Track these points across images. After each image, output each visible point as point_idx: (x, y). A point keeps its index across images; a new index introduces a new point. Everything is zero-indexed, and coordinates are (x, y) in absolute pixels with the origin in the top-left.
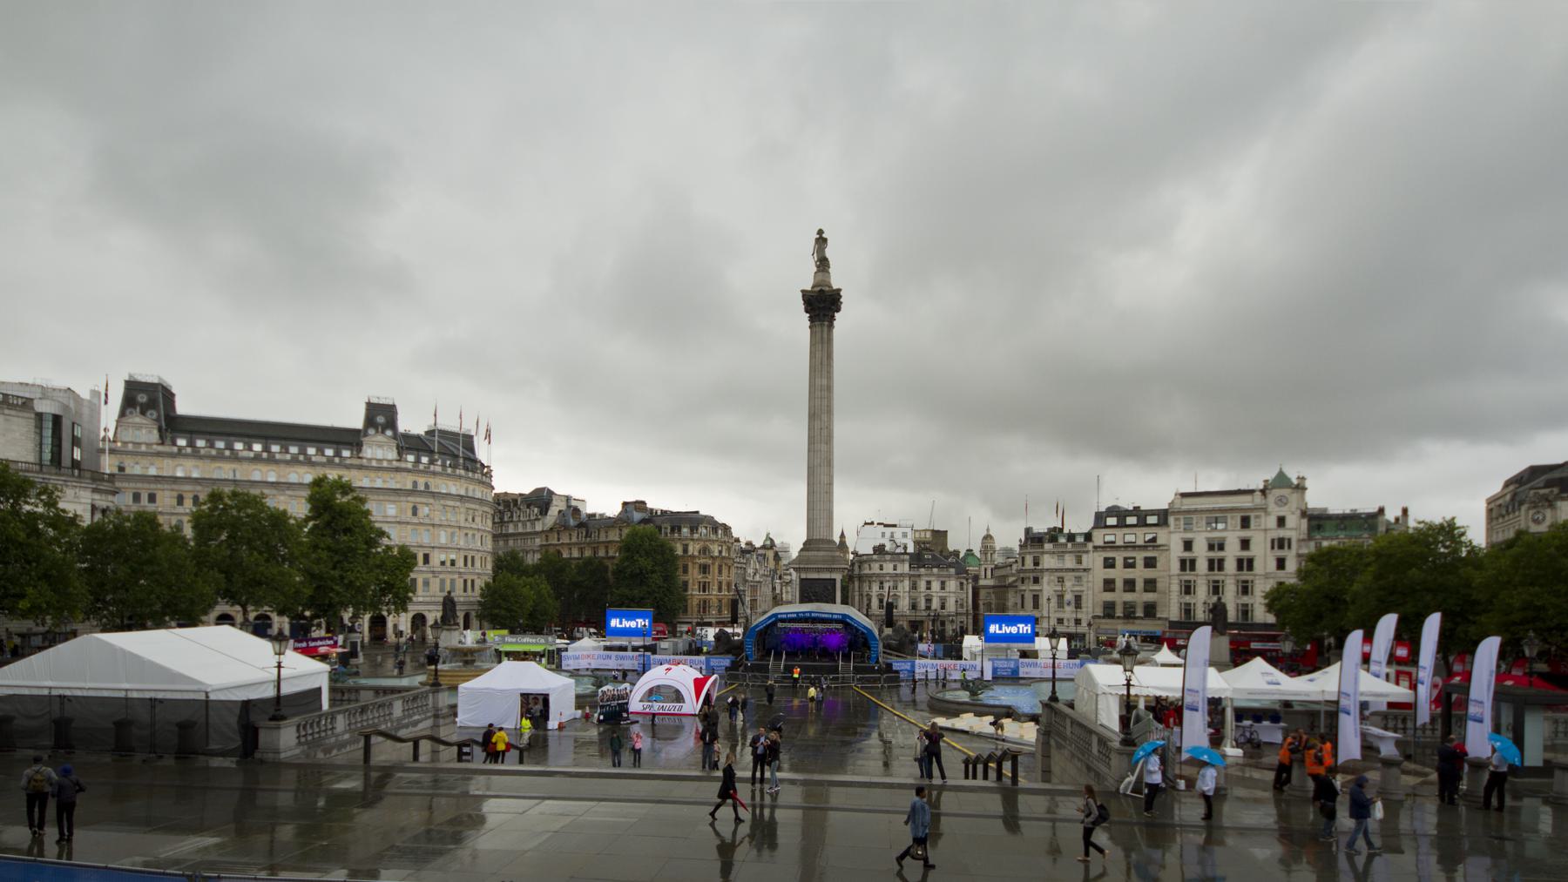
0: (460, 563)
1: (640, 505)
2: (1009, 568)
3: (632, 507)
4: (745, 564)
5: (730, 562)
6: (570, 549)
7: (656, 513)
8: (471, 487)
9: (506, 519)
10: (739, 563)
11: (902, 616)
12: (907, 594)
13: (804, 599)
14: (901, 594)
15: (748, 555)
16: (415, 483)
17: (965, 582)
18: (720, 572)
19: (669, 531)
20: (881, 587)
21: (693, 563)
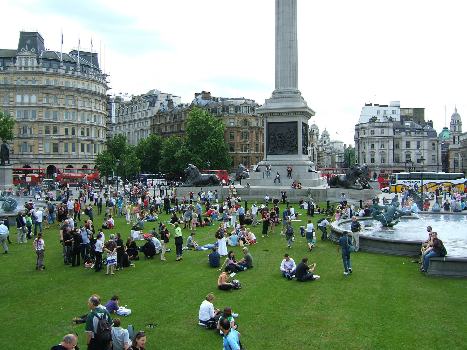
0: (79, 133)
1: (206, 95)
3: (199, 97)
6: (166, 127)
7: (217, 100)
8: (86, 84)
9: (133, 111)
11: (388, 167)
12: (392, 151)
14: (387, 151)
16: (48, 80)
17: (436, 143)
18: (257, 138)
19: (221, 110)
20: (373, 147)
21: (238, 132)
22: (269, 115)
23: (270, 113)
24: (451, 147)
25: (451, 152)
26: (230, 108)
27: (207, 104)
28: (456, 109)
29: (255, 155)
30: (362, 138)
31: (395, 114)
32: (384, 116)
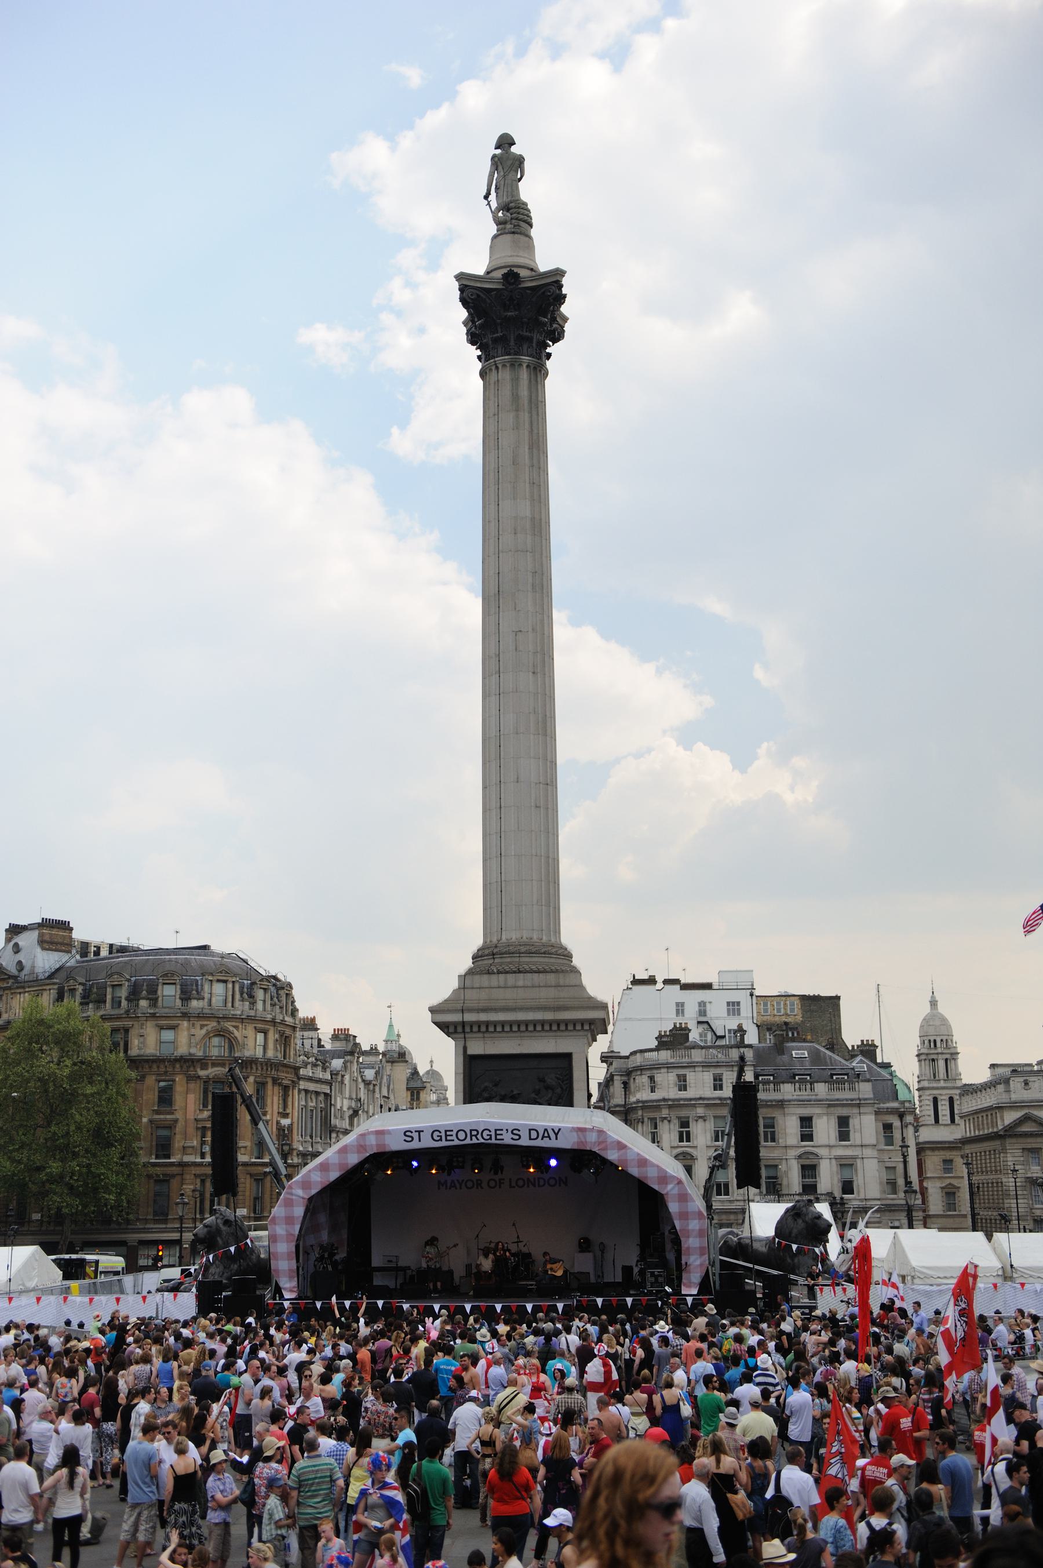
2: (1001, 1088)
4: (329, 1083)
5: (286, 1078)
7: (97, 953)
10: (310, 1079)
13: (472, 1094)
15: (337, 1063)
17: (897, 1123)
19: (123, 993)
20: (685, 1136)
21: (190, 1078)
22: (475, 1029)
23: (479, 1024)
24: (928, 1134)
25: (928, 1152)
26: (160, 987)
27: (58, 966)
28: (933, 996)
29: (249, 1168)
30: (647, 1106)
31: (739, 1014)
32: (699, 1022)
